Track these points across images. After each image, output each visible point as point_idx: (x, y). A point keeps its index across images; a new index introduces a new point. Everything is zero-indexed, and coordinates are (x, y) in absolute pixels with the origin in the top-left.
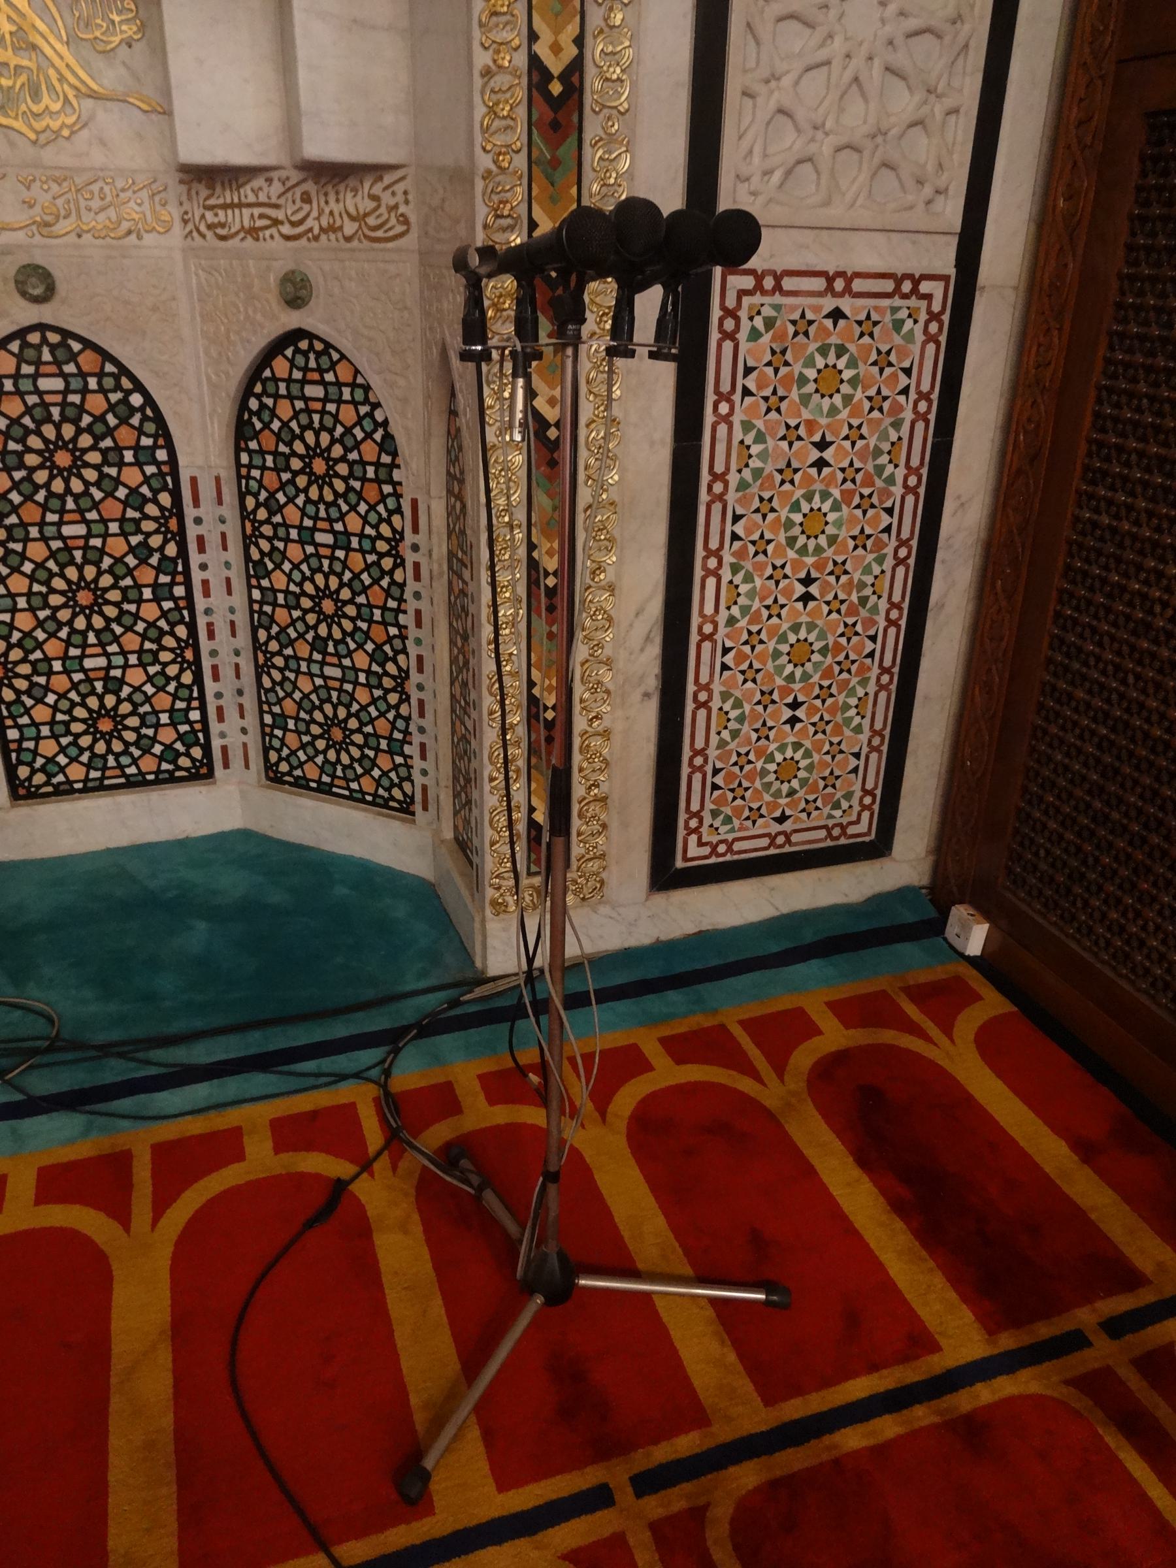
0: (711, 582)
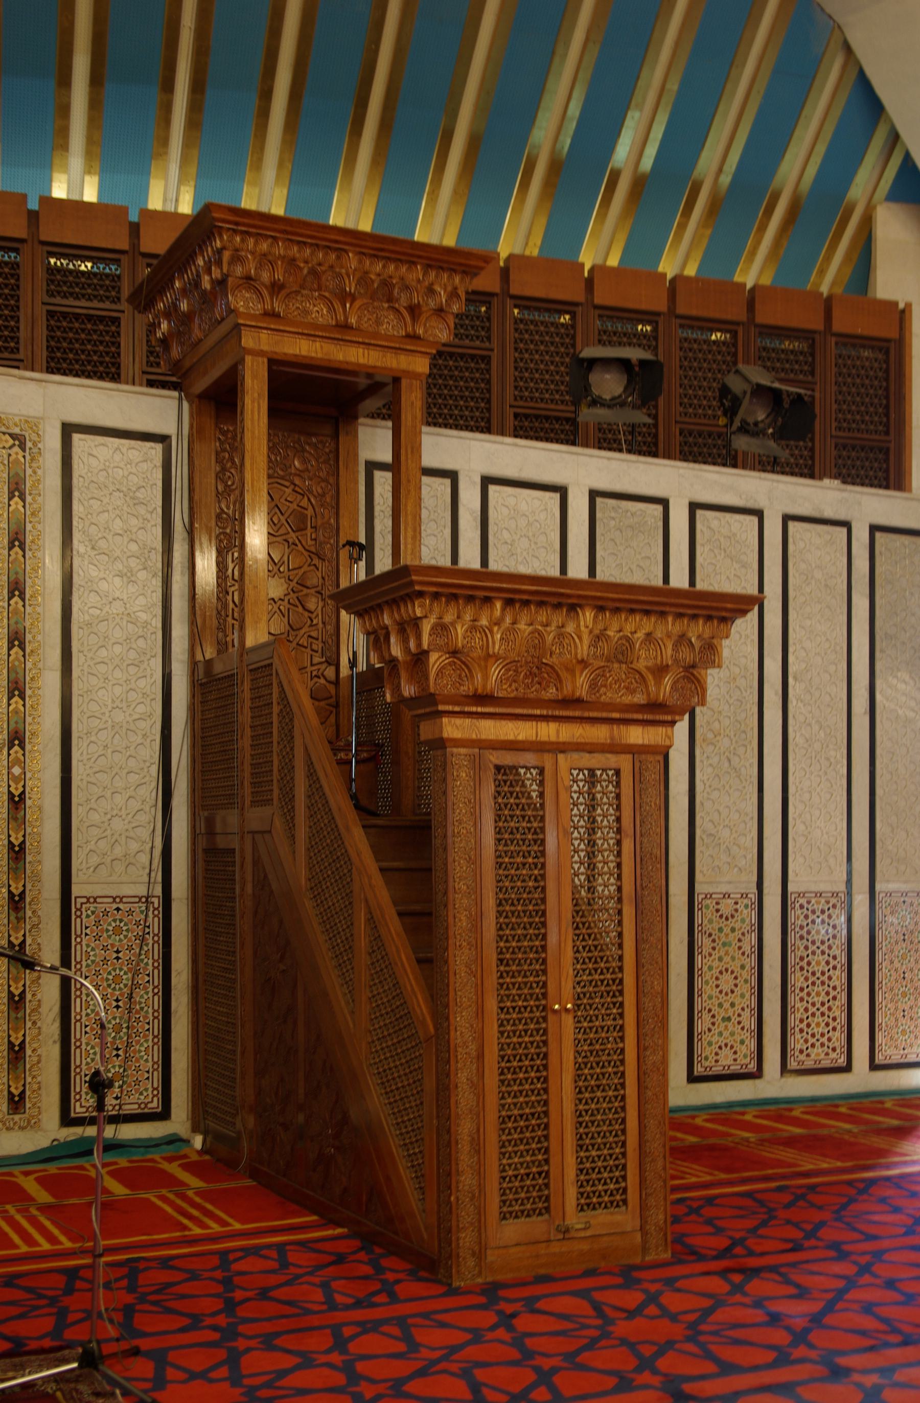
0: (78, 1000)
